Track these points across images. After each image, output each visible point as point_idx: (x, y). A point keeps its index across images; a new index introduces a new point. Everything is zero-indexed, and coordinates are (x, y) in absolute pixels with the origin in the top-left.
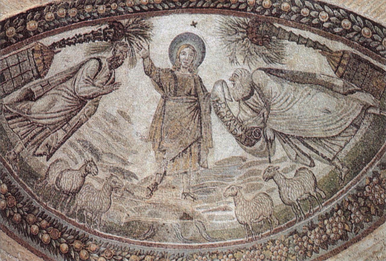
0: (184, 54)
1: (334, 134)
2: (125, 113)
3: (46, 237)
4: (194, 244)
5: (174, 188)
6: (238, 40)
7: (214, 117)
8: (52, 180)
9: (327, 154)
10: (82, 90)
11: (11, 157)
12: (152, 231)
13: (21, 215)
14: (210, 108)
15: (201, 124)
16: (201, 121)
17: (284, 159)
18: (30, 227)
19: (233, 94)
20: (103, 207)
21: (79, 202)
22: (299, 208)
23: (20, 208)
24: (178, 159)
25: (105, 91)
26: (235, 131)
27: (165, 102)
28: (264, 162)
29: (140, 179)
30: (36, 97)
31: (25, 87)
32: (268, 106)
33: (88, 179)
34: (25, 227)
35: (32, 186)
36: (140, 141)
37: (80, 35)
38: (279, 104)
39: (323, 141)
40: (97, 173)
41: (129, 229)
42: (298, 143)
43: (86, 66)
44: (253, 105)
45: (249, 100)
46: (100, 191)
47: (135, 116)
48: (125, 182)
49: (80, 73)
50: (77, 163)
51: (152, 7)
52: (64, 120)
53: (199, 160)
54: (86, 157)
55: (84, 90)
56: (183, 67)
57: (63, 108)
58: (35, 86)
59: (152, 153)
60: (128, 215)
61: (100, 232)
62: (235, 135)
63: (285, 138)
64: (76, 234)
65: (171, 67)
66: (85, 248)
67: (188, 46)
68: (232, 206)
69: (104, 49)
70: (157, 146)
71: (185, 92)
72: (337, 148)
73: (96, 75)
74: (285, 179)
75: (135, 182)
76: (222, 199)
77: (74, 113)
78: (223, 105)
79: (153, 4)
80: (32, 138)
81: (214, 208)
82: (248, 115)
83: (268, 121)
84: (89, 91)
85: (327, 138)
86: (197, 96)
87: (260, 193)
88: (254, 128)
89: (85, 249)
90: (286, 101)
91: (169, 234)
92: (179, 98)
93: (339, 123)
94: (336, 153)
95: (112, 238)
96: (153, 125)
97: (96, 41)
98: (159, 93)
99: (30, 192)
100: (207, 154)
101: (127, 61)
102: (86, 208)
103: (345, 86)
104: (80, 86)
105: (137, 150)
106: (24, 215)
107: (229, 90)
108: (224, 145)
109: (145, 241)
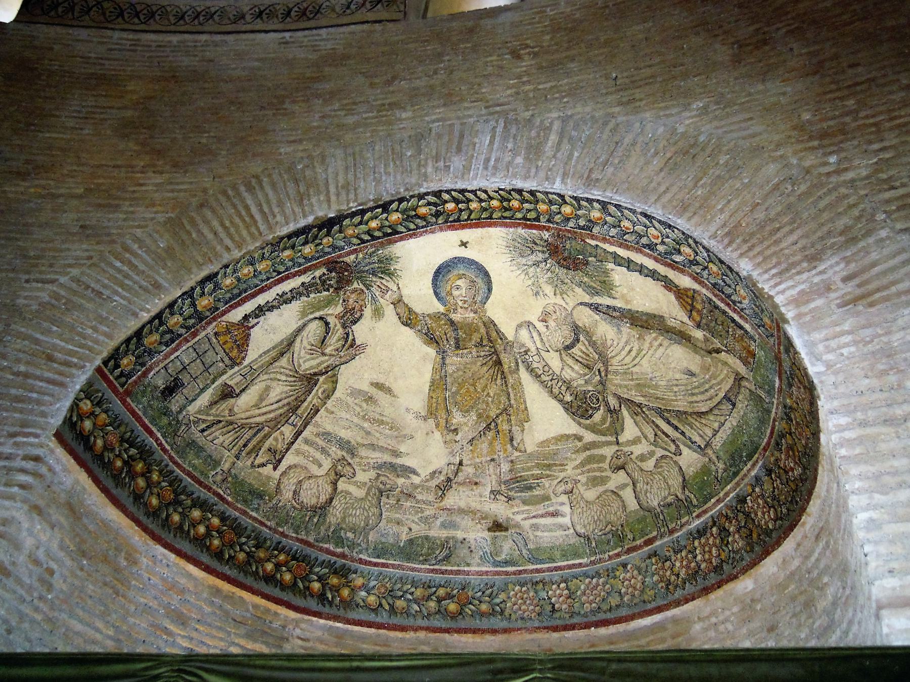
1: (704, 410)
3: (288, 577)
4: (510, 569)
5: (476, 484)
7: (524, 374)
8: (287, 494)
9: (697, 439)
10: (307, 365)
11: (219, 478)
12: (447, 550)
13: (247, 553)
14: (517, 363)
18: (262, 566)
19: (549, 341)
22: (661, 517)
23: (244, 544)
27: (443, 358)
28: (608, 443)
29: (423, 476)
30: (237, 391)
31: (217, 383)
33: (341, 485)
35: (257, 510)
36: (414, 421)
37: (284, 293)
38: (619, 358)
40: (354, 474)
41: (412, 550)
42: (656, 417)
43: (304, 333)
48: (401, 481)
50: (320, 466)
51: (389, 231)
53: (512, 440)
54: (333, 455)
57: (284, 395)
58: (232, 378)
59: (437, 435)
60: (410, 529)
61: (368, 559)
62: (561, 401)
63: (636, 409)
64: (330, 565)
65: (442, 309)
68: (566, 509)
69: (329, 303)
72: (709, 433)
74: (642, 470)
75: (416, 480)
77: (302, 398)
78: (536, 358)
79: (390, 227)
80: (245, 446)
81: (540, 512)
82: (577, 373)
84: (319, 364)
87: (606, 491)
88: (589, 391)
90: (630, 351)
91: (473, 555)
92: (465, 351)
93: (708, 394)
97: (312, 295)
99: (255, 519)
100: (523, 431)
101: (368, 312)
102: (344, 526)
103: (706, 340)
104: (301, 361)
106: (251, 551)
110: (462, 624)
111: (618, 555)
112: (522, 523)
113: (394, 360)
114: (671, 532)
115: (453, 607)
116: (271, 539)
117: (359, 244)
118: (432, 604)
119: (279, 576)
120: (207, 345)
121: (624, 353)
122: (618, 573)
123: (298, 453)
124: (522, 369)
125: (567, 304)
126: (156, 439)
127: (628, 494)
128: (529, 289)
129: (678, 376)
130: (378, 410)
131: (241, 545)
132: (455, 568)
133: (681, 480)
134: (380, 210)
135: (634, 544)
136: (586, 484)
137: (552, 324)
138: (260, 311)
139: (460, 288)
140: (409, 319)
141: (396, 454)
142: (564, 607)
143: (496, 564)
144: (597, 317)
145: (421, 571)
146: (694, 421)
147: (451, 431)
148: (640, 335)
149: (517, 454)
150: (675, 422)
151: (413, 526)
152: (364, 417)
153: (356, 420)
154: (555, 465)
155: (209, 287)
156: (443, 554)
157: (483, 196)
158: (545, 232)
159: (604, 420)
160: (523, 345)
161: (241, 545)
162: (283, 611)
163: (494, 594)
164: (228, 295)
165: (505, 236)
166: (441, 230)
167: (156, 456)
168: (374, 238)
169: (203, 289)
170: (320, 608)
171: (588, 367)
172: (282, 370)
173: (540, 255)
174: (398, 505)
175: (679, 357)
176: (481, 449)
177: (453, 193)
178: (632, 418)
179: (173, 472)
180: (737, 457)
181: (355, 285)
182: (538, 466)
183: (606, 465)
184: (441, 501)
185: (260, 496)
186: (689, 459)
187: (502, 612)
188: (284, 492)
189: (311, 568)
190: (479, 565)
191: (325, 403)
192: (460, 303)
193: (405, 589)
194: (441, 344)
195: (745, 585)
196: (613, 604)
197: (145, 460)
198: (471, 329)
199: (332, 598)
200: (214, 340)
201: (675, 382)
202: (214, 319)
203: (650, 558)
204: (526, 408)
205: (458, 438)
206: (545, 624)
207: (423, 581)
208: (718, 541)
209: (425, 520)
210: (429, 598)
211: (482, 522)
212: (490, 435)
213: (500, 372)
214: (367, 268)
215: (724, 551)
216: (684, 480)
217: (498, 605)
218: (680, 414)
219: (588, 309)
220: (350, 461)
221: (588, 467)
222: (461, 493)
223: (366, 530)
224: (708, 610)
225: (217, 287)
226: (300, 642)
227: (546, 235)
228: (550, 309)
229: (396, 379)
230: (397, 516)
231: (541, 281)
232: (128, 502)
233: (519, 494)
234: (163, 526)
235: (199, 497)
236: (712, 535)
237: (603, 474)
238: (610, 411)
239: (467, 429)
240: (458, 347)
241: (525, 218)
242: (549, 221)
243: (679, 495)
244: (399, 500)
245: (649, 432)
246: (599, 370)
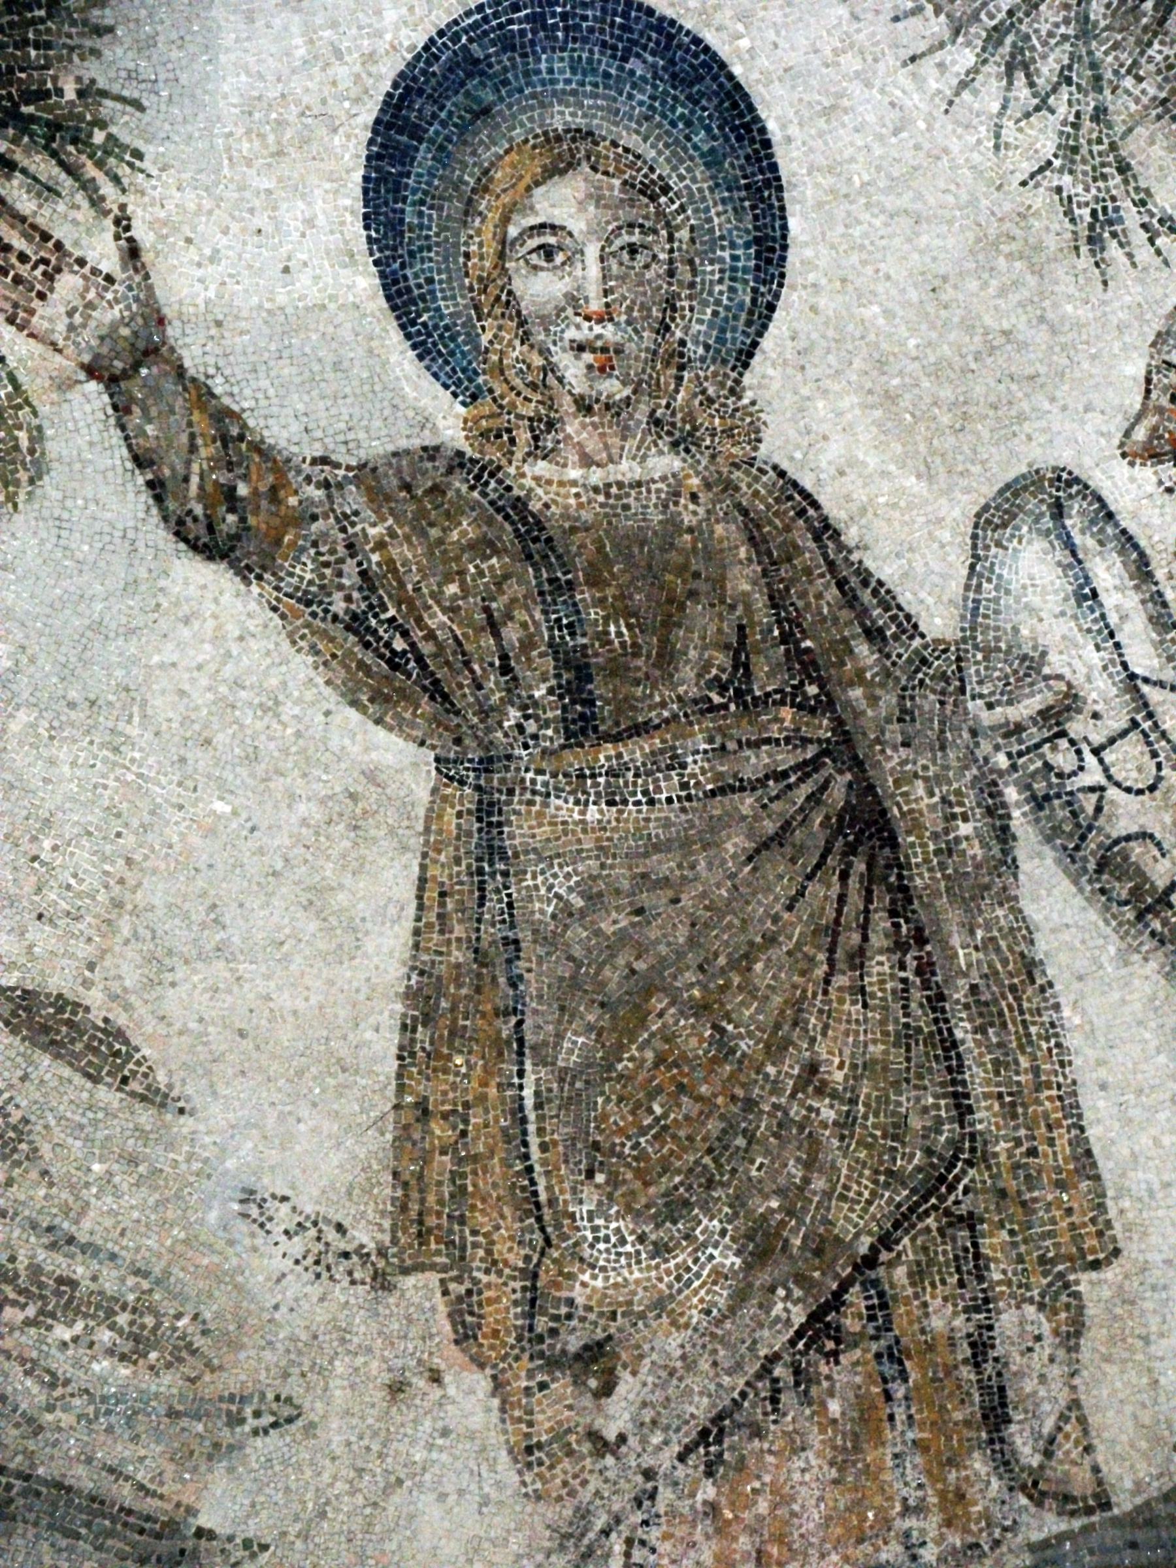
0: (551, 246)
7: (1054, 905)
14: (996, 811)
15: (937, 1000)
16: (925, 969)
24: (757, 1432)
27: (488, 812)
36: (300, 1285)
53: (996, 1414)
56: (584, 406)
59: (469, 1397)
65: (449, 422)
67: (562, 155)
70: (503, 1307)
71: (687, 681)
78: (1129, 760)
86: (827, 704)
92: (636, 751)
96: (434, 1090)
98: (400, 727)
100: (1072, 1335)
105: (293, 1388)
128: (1040, 198)
130: (32, 1194)
140: (225, 500)
147: (553, 1363)
160: (1031, 666)
176: (782, 1498)
194: (465, 697)
198: (655, 570)
204: (1085, 1160)
205: (616, 1417)
212: (846, 1376)
213: (882, 900)
229: (159, 966)
231: (1122, 108)
239: (674, 1343)
240: (581, 728)
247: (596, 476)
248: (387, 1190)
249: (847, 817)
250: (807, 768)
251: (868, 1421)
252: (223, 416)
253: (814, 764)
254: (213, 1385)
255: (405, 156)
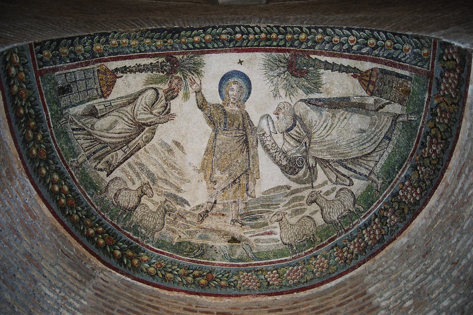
0: (232, 90)
1: (369, 152)
2: (179, 143)
3: (102, 242)
4: (240, 263)
5: (223, 215)
6: (279, 75)
11: (74, 164)
12: (202, 251)
13: (80, 217)
14: (257, 141)
16: (249, 154)
17: (325, 183)
18: (87, 229)
19: (278, 126)
20: (157, 227)
21: (134, 219)
23: (79, 211)
25: (161, 120)
26: (281, 162)
27: (216, 135)
28: (307, 188)
30: (99, 115)
31: (90, 103)
32: (309, 134)
33: (144, 200)
34: (82, 228)
35: (92, 196)
36: (192, 171)
38: (319, 132)
39: (360, 160)
43: (145, 95)
44: (296, 136)
45: (292, 132)
46: (155, 212)
47: (187, 147)
48: (178, 207)
49: (139, 100)
50: (134, 184)
51: (204, 45)
52: (124, 141)
53: (247, 190)
54: (143, 179)
55: (143, 117)
56: (232, 103)
57: (123, 131)
58: (99, 104)
59: (204, 183)
60: (180, 237)
61: (152, 247)
63: (325, 163)
64: (128, 243)
65: (221, 102)
66: (138, 257)
67: (235, 83)
68: (278, 230)
69: (161, 81)
70: (208, 177)
72: (372, 164)
73: (154, 104)
74: (327, 200)
75: (188, 208)
76: (268, 225)
77: (133, 137)
78: (269, 138)
79: (204, 43)
80: (94, 153)
81: (261, 232)
82: (292, 146)
83: (310, 150)
85: (363, 156)
86: (245, 131)
87: (303, 217)
88: (298, 157)
89: (138, 259)
90: (325, 127)
91: (217, 255)
93: (373, 141)
94: (371, 169)
95: (163, 253)
97: (154, 73)
98: (210, 126)
99: (88, 200)
100: (255, 185)
101: (181, 93)
102: (141, 225)
104: (138, 112)
105: (190, 179)
106: (82, 217)
107: (273, 123)
108: (270, 176)
109: (194, 259)
110: (208, 291)
111: (311, 251)
112: (249, 238)
113: (188, 130)
114: (346, 231)
115: (203, 281)
116: (96, 216)
117: (186, 49)
118: (190, 279)
119: (96, 239)
120: (92, 75)
121: (322, 128)
122: (311, 262)
123: (123, 171)
124: (260, 145)
125: (292, 101)
126: (48, 114)
127: (318, 218)
128: (271, 93)
129: (353, 136)
131: (77, 211)
132: (206, 261)
133: (352, 199)
134: (201, 31)
135: (321, 243)
136: (291, 214)
137: (281, 115)
138: (125, 70)
139: (234, 89)
140: (202, 105)
141: (179, 190)
142: (275, 283)
143: (231, 260)
144: (309, 108)
145: (185, 260)
146: (362, 161)
147: (212, 182)
148: (333, 114)
149: (249, 199)
150: (350, 166)
151: (182, 235)
152: (165, 161)
153: (160, 161)
154: (272, 205)
155: (103, 39)
156: (200, 252)
157: (257, 30)
158: (288, 53)
159: (305, 175)
160: (262, 130)
161: (77, 211)
162: (94, 260)
163: (230, 276)
164: (111, 51)
165: (264, 58)
166: (230, 51)
167: (43, 125)
168: (195, 48)
169: (100, 38)
170: (118, 266)
171: (299, 141)
172: (127, 114)
173: (282, 69)
174: (174, 222)
175: (357, 121)
177: (242, 27)
178: (323, 170)
179: (51, 142)
180: (389, 172)
181: (178, 75)
182: (262, 206)
183: (304, 202)
184: (201, 223)
185: (96, 188)
186: (359, 186)
187: (235, 286)
188: (110, 192)
189: (117, 242)
190: (221, 260)
191: (145, 145)
192: (232, 100)
193: (173, 268)
194: (216, 125)
195: (402, 240)
196: (308, 278)
197: (37, 123)
198: (234, 118)
199: (127, 263)
200: (96, 74)
201: (352, 140)
202: (100, 61)
203: (332, 249)
206: (264, 292)
207: (185, 265)
208: (379, 225)
209: (190, 233)
210: (188, 275)
211: (225, 237)
212: (236, 186)
213: (246, 147)
214: (187, 66)
215: (384, 229)
216: (355, 198)
217: (232, 282)
218: (355, 160)
219: (304, 103)
220: (151, 186)
221: (293, 204)
222: (213, 220)
223: (153, 231)
224: (375, 267)
225: (107, 42)
226: (102, 281)
227: (288, 55)
228: (281, 106)
230: (173, 227)
232: (20, 140)
233: (249, 222)
234: (35, 171)
235: (60, 168)
236: (375, 223)
237: (302, 207)
238: (309, 168)
239: (222, 181)
241: (278, 45)
242: (291, 46)
243: (351, 209)
244: (176, 218)
245: (333, 177)
246: (305, 143)
247: (231, 109)
248: (201, 165)
249: (245, 140)
250: (242, 136)
251: (237, 189)
252: (204, 98)
253: (243, 135)
254: (184, 178)
255: (223, 81)
